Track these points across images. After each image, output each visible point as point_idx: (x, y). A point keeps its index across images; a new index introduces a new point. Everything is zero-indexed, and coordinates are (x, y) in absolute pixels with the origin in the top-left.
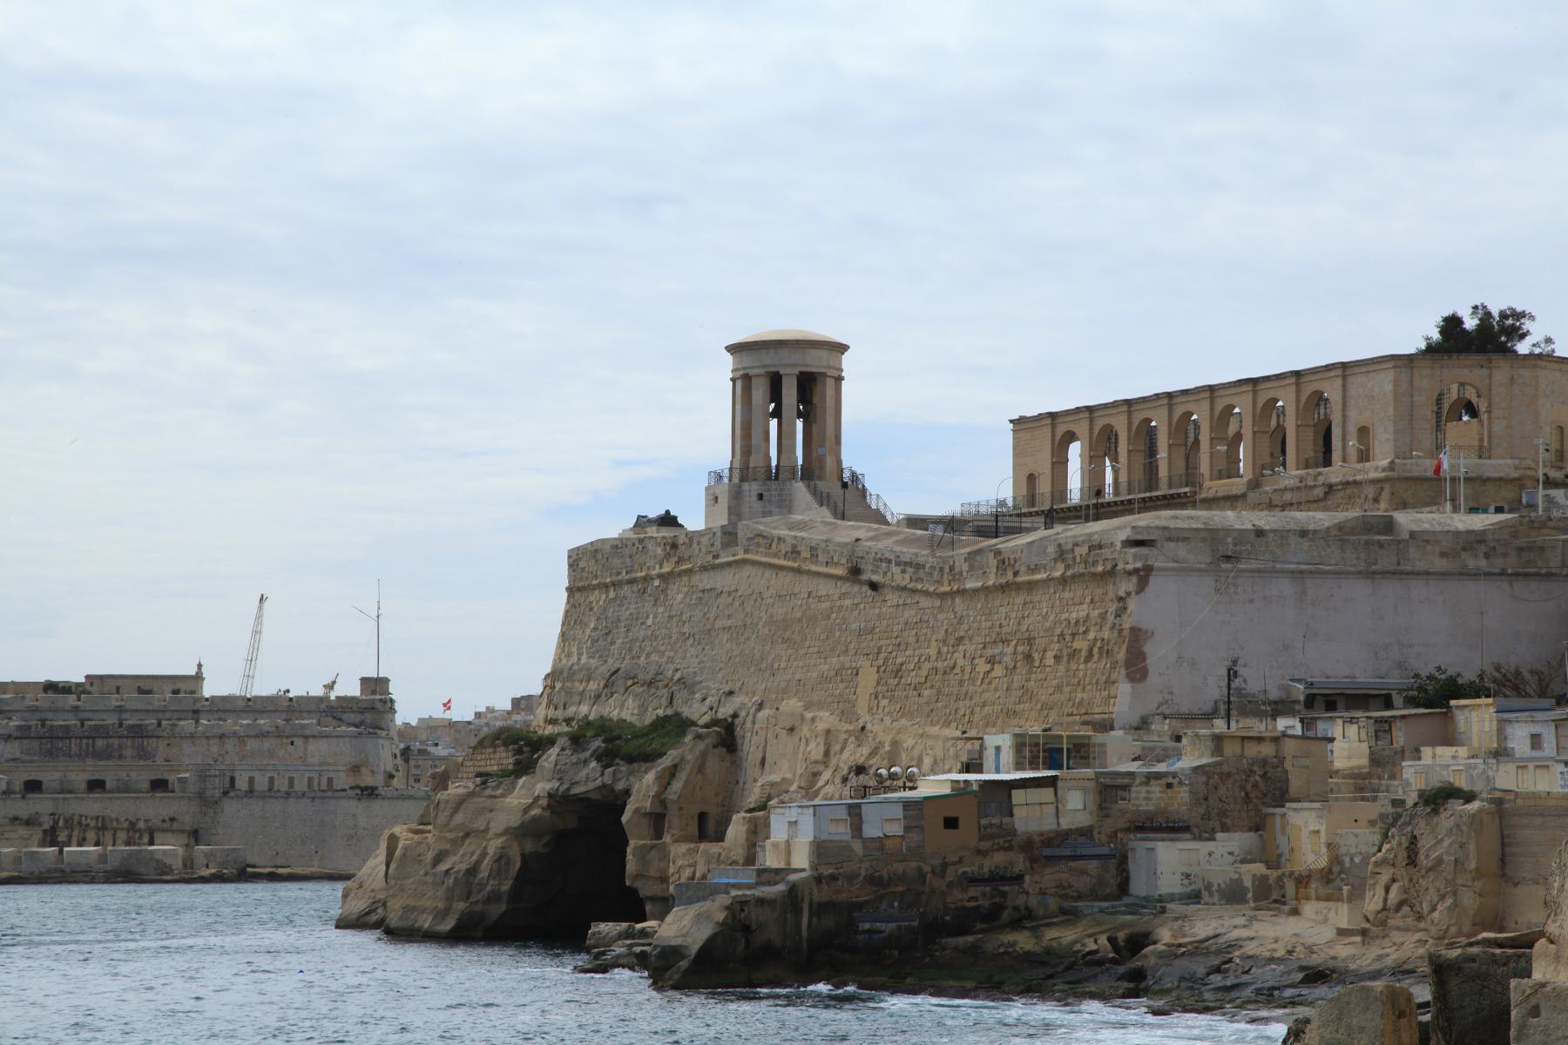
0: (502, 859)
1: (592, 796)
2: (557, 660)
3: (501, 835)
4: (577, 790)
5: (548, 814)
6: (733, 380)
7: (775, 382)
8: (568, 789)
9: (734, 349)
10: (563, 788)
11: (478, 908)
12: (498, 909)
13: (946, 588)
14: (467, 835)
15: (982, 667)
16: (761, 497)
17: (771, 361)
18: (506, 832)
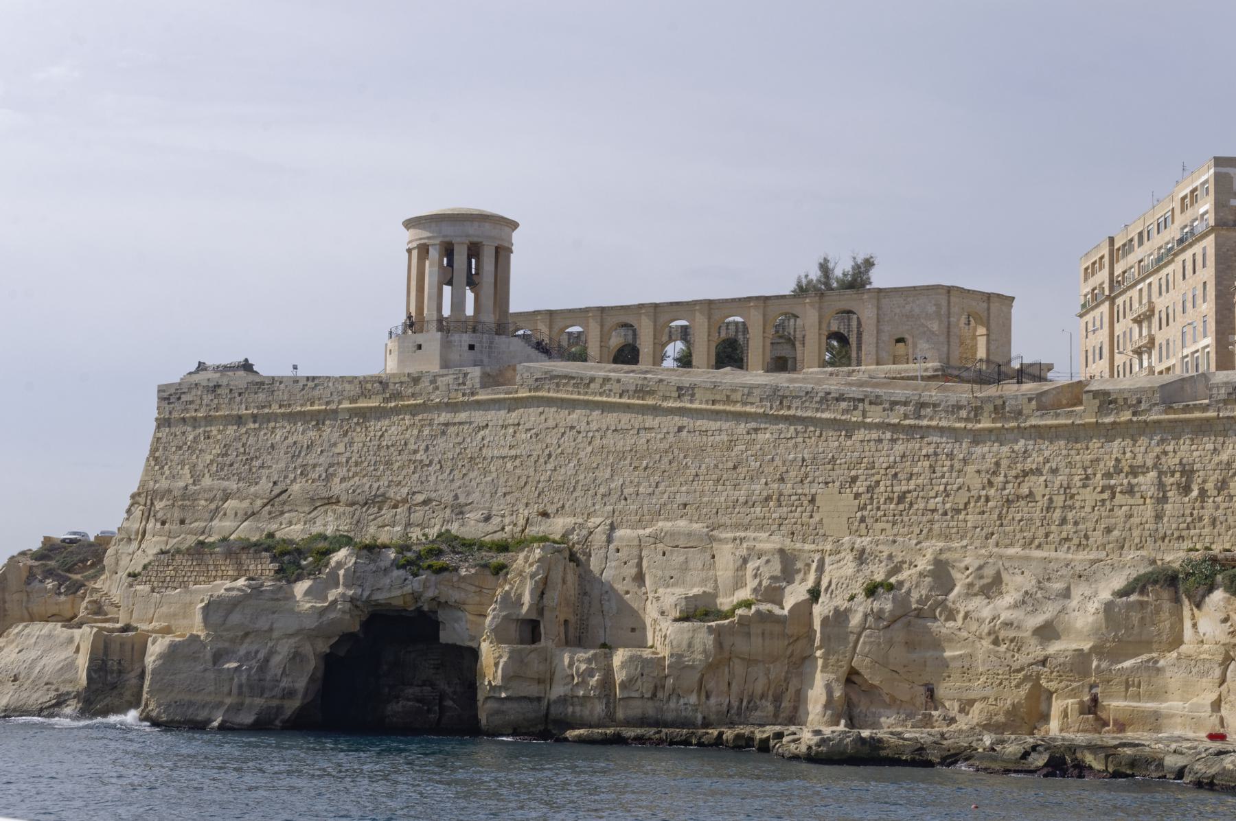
0: (296, 657)
1: (394, 602)
2: (143, 483)
3: (290, 636)
4: (380, 597)
5: (347, 617)
6: (409, 251)
7: (474, 250)
8: (370, 596)
9: (410, 224)
10: (366, 594)
11: (275, 703)
12: (294, 704)
13: (985, 424)
14: (247, 634)
15: (1089, 496)
16: (472, 347)
17: (449, 231)
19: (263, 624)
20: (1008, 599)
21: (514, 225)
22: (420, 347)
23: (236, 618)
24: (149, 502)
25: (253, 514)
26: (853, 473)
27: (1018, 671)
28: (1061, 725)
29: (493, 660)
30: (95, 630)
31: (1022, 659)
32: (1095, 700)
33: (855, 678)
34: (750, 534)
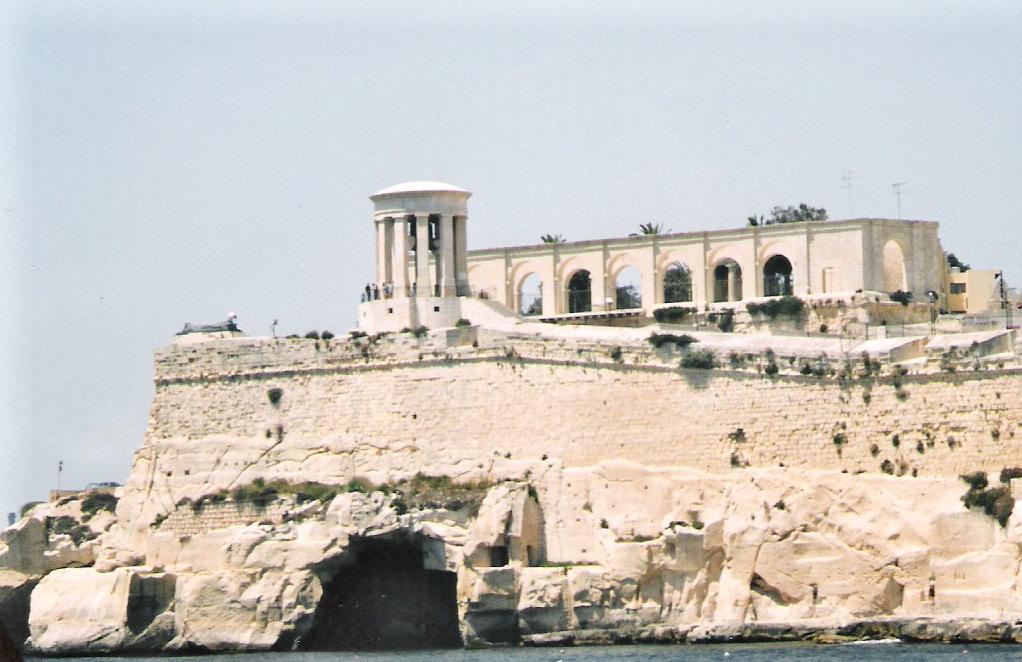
1: (385, 538)
18: (308, 566)
19: (276, 561)
20: (870, 515)
21: (467, 195)
22: (391, 311)
23: (253, 557)
24: (154, 457)
25: (252, 463)
26: (755, 415)
27: (877, 570)
28: (910, 611)
29: (471, 585)
30: (131, 573)
31: (881, 561)
32: (932, 593)
33: (759, 582)
34: (674, 468)
